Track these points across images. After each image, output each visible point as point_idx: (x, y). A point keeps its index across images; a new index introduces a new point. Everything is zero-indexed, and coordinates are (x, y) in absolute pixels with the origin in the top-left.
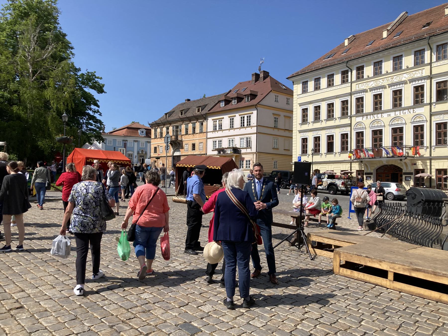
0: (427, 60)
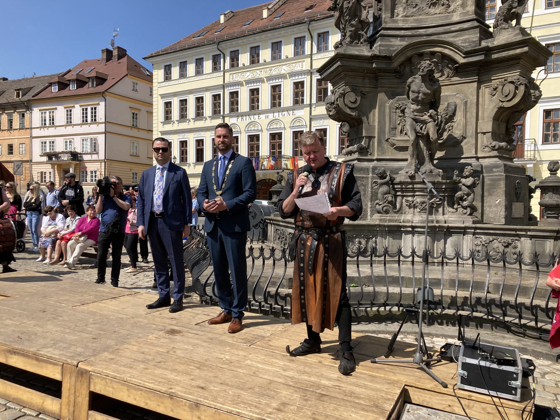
0: (308, 51)
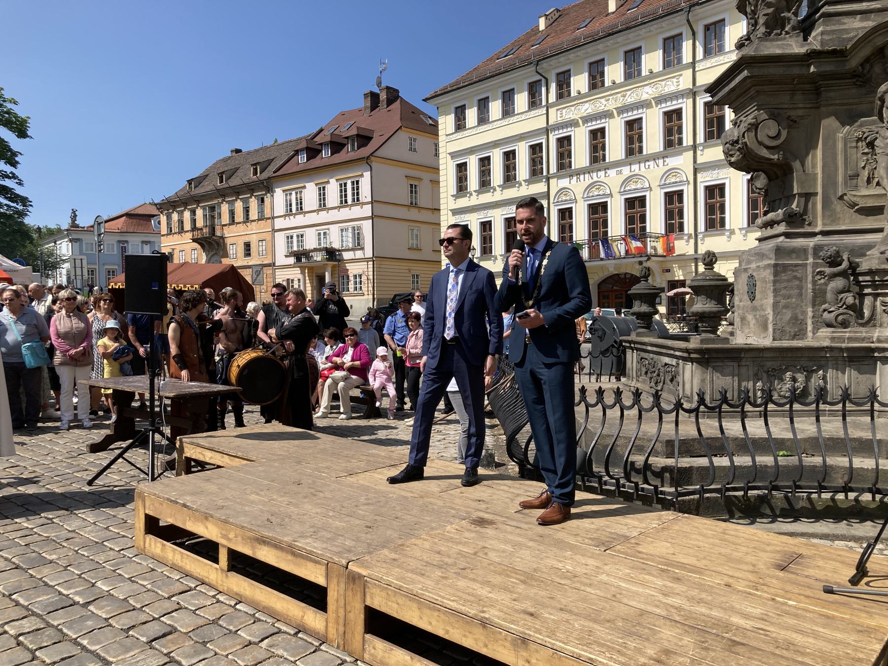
0: (687, 58)
